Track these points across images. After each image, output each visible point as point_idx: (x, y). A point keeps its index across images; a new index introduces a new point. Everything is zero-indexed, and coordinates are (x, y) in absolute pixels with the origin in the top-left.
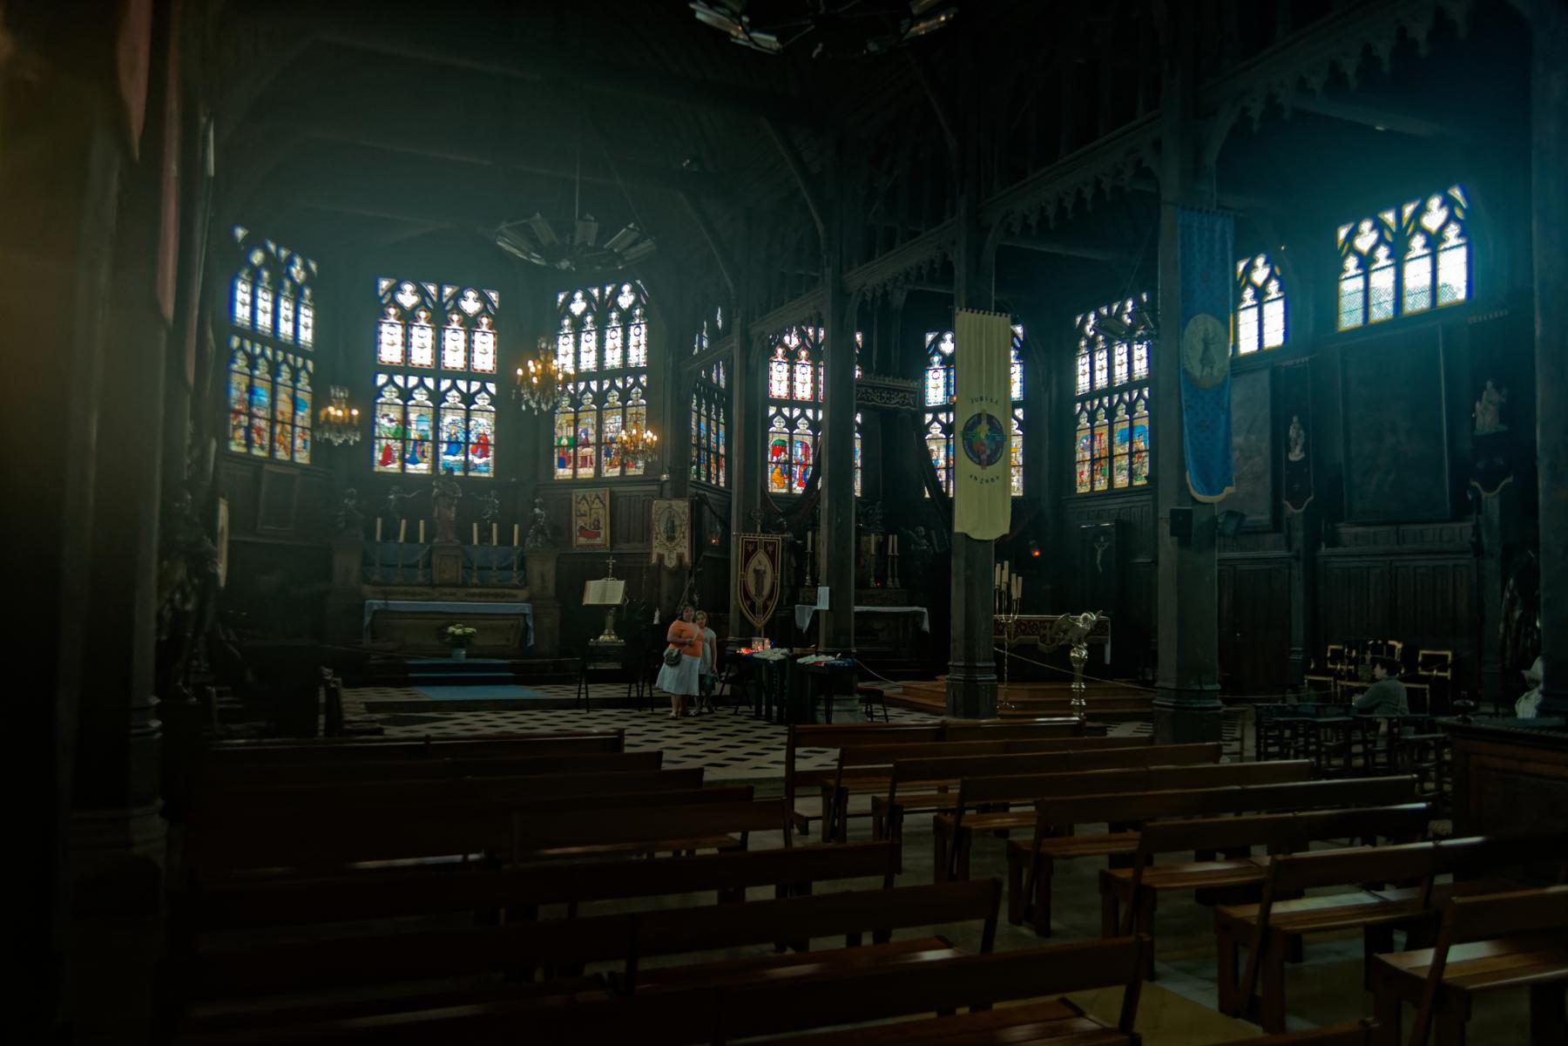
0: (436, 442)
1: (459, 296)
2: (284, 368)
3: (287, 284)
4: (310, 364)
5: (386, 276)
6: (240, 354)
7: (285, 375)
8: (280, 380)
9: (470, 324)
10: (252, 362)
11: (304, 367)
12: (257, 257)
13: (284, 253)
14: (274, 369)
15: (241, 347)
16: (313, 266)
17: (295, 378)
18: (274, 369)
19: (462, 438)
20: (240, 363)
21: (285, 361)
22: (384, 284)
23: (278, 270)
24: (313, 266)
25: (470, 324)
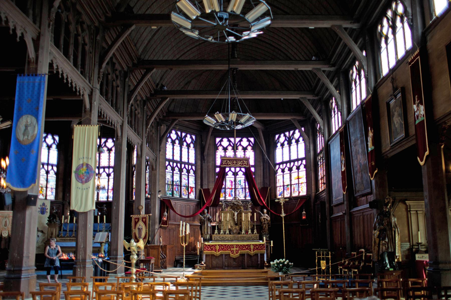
0: (235, 189)
1: (241, 141)
2: (184, 170)
4: (194, 167)
5: (219, 137)
6: (169, 167)
8: (183, 173)
9: (245, 149)
10: (173, 169)
11: (192, 168)
12: (173, 136)
13: (184, 134)
14: (181, 170)
15: (169, 164)
17: (188, 172)
19: (244, 186)
20: (169, 168)
21: (185, 167)
22: (218, 140)
23: (181, 141)
24: (194, 137)
25: (245, 149)
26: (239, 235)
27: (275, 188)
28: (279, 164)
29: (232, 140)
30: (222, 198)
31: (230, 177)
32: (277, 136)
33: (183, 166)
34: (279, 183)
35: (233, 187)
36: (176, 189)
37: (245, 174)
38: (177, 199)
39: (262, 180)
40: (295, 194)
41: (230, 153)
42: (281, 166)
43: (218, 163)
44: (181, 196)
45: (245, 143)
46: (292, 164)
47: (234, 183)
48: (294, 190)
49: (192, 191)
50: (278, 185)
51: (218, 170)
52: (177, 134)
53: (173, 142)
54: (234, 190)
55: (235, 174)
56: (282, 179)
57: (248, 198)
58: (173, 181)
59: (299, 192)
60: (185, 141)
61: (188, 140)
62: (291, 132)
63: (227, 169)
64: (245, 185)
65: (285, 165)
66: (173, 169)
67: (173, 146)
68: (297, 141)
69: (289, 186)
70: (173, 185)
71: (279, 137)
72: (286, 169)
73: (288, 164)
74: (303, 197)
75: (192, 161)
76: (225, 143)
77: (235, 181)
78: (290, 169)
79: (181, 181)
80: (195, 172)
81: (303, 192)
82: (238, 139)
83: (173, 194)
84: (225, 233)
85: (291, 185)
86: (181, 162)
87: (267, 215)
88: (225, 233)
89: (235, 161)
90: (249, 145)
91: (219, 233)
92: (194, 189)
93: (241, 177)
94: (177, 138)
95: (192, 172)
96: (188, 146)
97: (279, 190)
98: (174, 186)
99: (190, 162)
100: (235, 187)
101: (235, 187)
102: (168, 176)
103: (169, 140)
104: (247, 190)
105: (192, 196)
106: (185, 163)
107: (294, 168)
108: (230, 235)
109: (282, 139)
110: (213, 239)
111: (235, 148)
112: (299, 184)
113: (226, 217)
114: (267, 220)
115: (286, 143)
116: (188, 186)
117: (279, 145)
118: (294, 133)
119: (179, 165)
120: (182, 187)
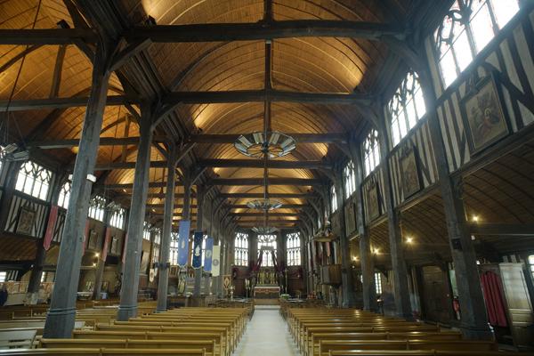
12: (238, 235)
20: (236, 253)
23: (242, 237)
31: (264, 255)
34: (288, 258)
41: (265, 244)
43: (259, 248)
55: (267, 254)
56: (289, 257)
61: (245, 237)
75: (247, 247)
76: (262, 237)
81: (299, 264)
89: (267, 248)
93: (270, 255)
97: (288, 262)
100: (267, 261)
101: (267, 261)
102: (236, 257)
105: (247, 265)
109: (290, 237)
113: (262, 275)
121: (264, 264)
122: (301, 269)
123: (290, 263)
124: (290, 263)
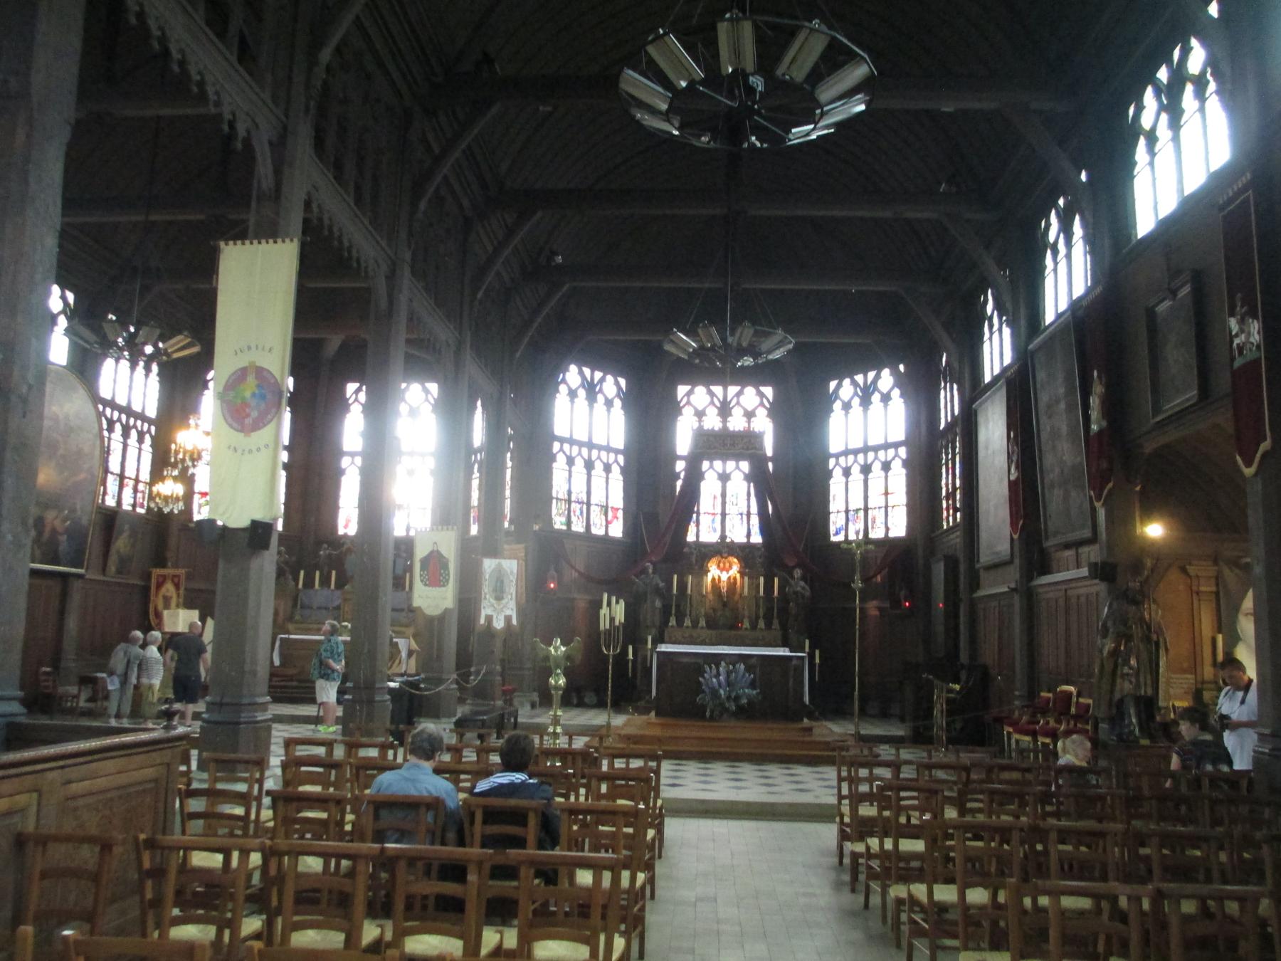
0: (724, 515)
1: (738, 394)
3: (600, 398)
4: (621, 459)
7: (599, 468)
8: (593, 472)
10: (570, 461)
11: (616, 461)
13: (598, 375)
14: (589, 465)
15: (561, 450)
16: (622, 382)
18: (589, 465)
20: (561, 461)
21: (599, 458)
22: (682, 390)
23: (592, 390)
26: (733, 632)
27: (826, 514)
28: (837, 456)
29: (718, 390)
30: (691, 537)
32: (833, 384)
33: (595, 453)
34: (836, 504)
35: (719, 510)
36: (578, 513)
37: (748, 478)
38: (577, 535)
39: (794, 493)
40: (877, 533)
41: (713, 422)
42: (842, 460)
44: (588, 526)
45: (750, 397)
46: (871, 455)
47: (719, 500)
48: (874, 522)
49: (616, 517)
50: (832, 507)
51: (680, 466)
52: (581, 373)
53: (573, 394)
54: (719, 518)
55: (724, 478)
57: (757, 538)
58: (570, 493)
59: (887, 529)
60: (601, 391)
62: (871, 375)
63: (705, 465)
64: (749, 506)
65: (851, 458)
66: (570, 461)
67: (572, 401)
68: (886, 398)
69: (861, 514)
70: (569, 501)
71: (839, 386)
72: (856, 470)
73: (861, 457)
74: (897, 540)
75: (619, 441)
77: (724, 495)
78: (866, 469)
79: (589, 493)
80: (624, 471)
81: (899, 529)
82: (732, 390)
83: (569, 523)
84: (695, 624)
85: (866, 510)
86: (590, 445)
87: (802, 583)
88: (695, 624)
90: (762, 404)
91: (680, 622)
92: (620, 514)
94: (582, 385)
95: (616, 470)
96: (609, 403)
98: (573, 505)
99: (613, 445)
101: (727, 511)
103: (563, 388)
104: (755, 520)
105: (617, 530)
106: (600, 448)
107: (877, 467)
108: (709, 632)
110: (666, 638)
111: (725, 410)
112: (886, 507)
114: (803, 596)
115: (856, 401)
116: (607, 507)
117: (837, 406)
118: (878, 377)
119: (585, 451)
120: (593, 508)
121: (703, 531)
122: (897, 561)
123: (843, 525)
124: (843, 525)
